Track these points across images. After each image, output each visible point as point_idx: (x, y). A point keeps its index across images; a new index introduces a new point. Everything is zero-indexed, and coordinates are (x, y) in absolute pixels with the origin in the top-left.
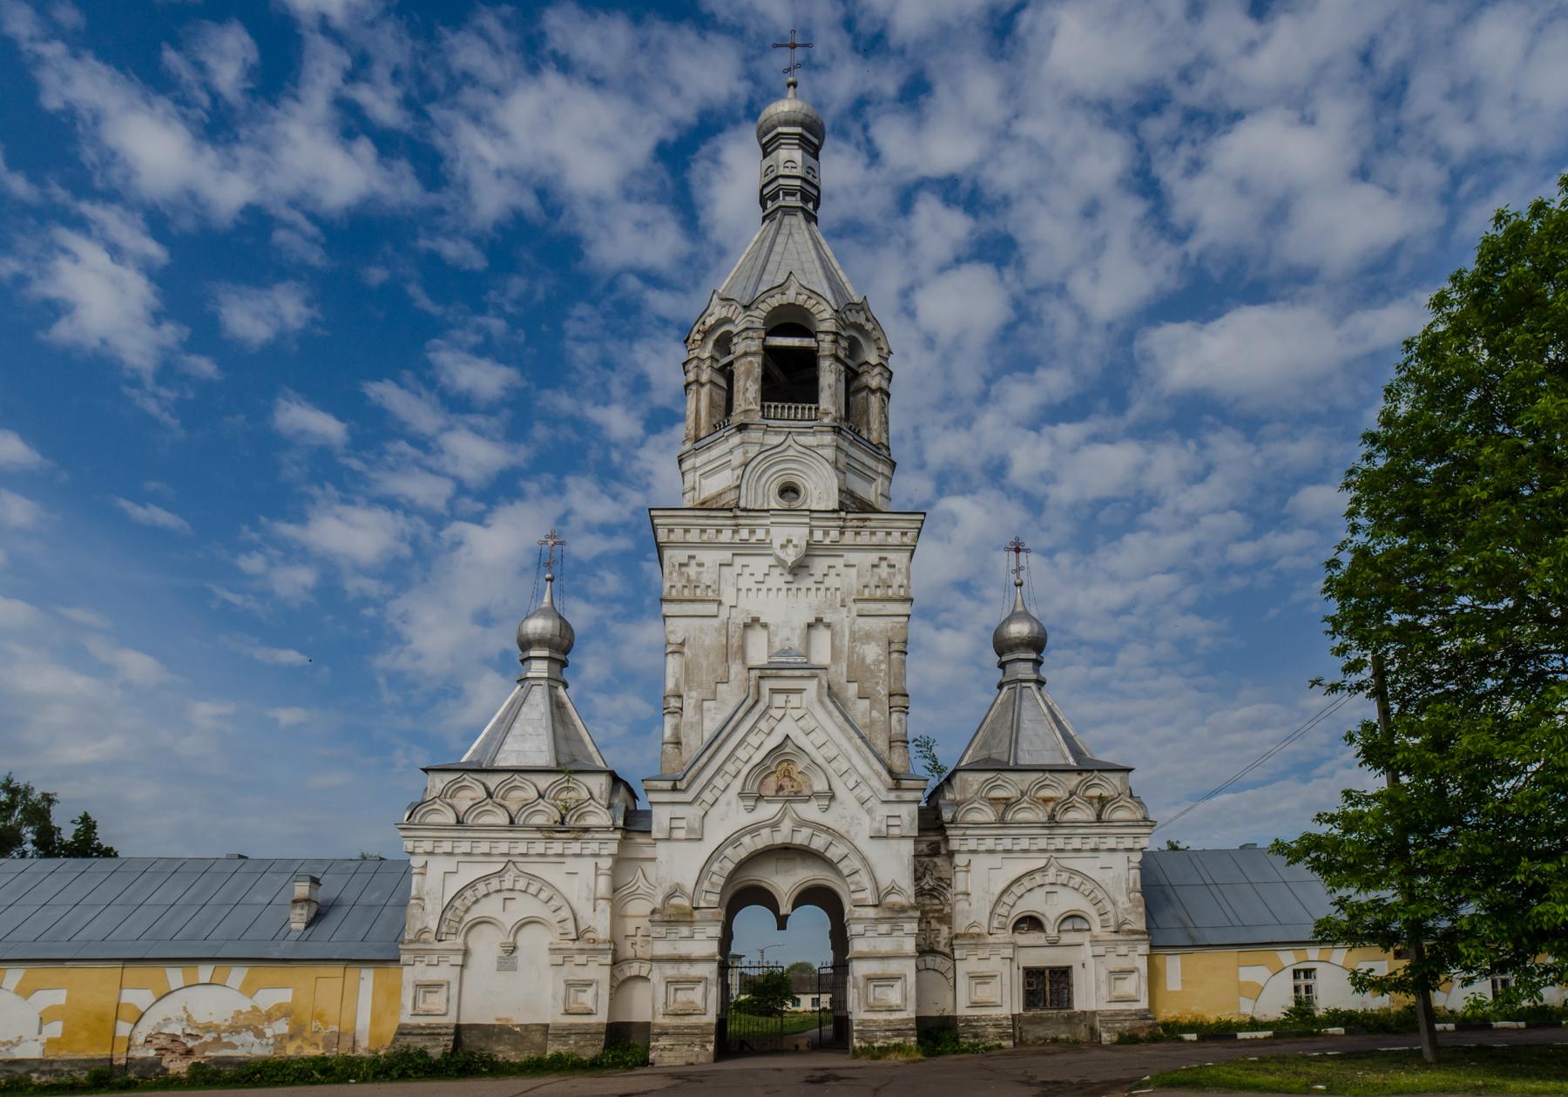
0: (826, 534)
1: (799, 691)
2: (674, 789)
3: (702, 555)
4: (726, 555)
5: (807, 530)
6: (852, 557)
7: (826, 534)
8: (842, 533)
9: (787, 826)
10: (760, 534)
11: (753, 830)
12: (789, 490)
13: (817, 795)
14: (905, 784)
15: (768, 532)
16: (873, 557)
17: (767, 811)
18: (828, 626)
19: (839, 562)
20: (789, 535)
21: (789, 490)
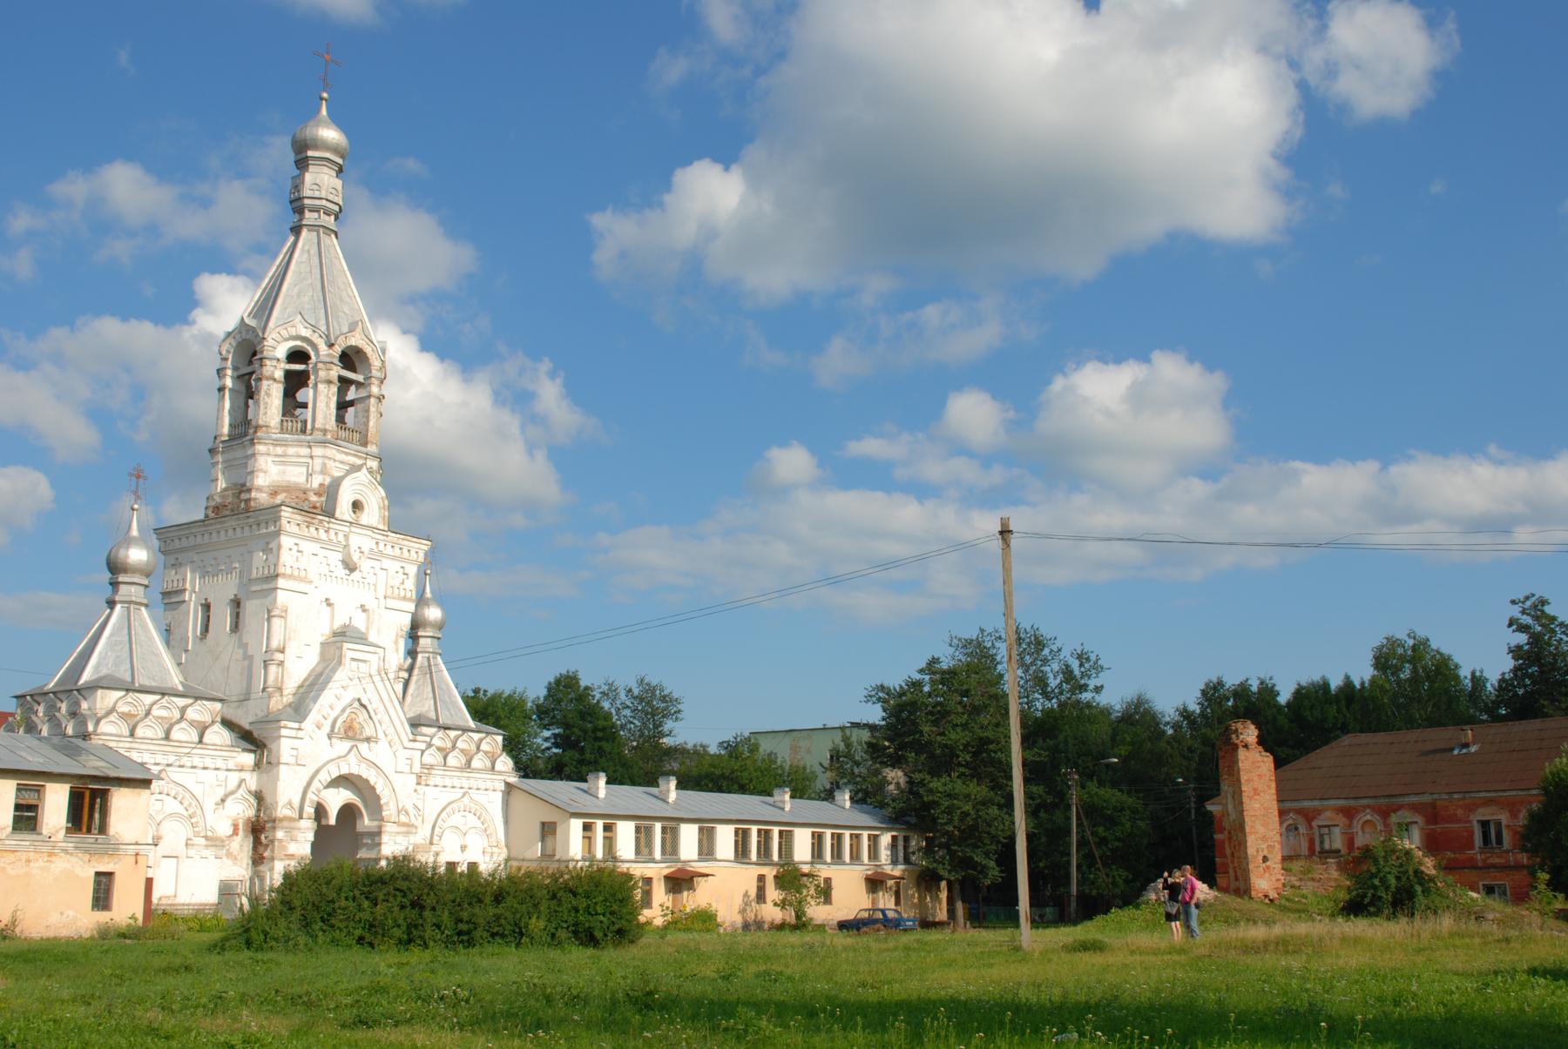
3: (304, 545)
4: (315, 547)
6: (386, 563)
12: (357, 506)
13: (368, 740)
15: (346, 537)
16: (397, 565)
17: (343, 746)
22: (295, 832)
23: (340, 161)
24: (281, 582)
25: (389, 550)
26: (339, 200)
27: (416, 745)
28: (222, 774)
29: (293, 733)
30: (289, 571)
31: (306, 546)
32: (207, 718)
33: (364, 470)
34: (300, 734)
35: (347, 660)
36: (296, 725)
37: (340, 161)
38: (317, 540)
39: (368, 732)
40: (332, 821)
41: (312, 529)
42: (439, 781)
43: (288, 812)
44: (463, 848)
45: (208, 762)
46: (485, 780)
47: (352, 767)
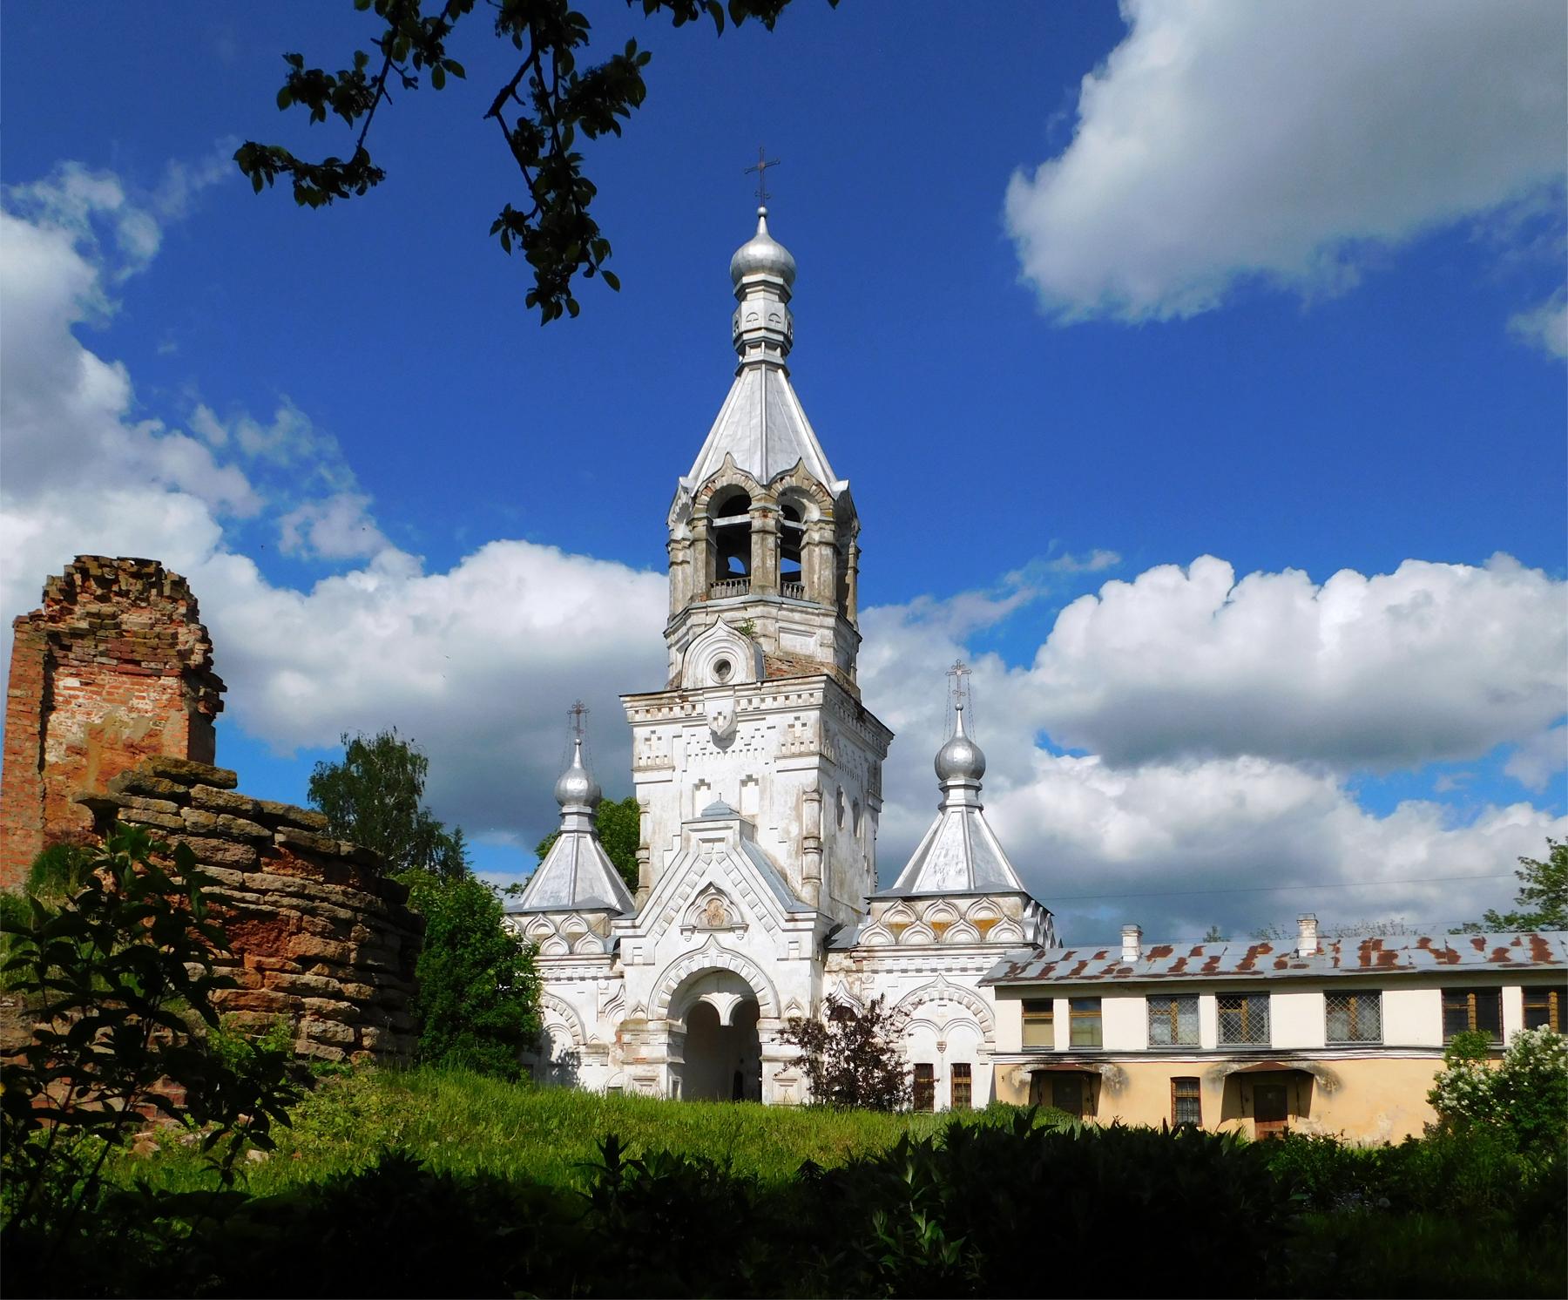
0: (750, 701)
1: (721, 840)
2: (634, 927)
5: (731, 701)
6: (771, 719)
7: (750, 701)
8: (763, 700)
9: (713, 952)
10: (699, 708)
11: (690, 954)
12: (723, 666)
14: (798, 916)
18: (756, 781)
19: (762, 725)
20: (717, 706)
21: (723, 666)
22: (644, 1036)
23: (780, 281)
24: (638, 777)
25: (769, 703)
26: (783, 327)
27: (800, 925)
28: (603, 983)
29: (630, 932)
30: (642, 763)
31: (666, 731)
32: (583, 929)
33: (720, 624)
34: (639, 932)
35: (693, 842)
36: (628, 923)
37: (780, 281)
38: (675, 721)
39: (736, 918)
40: (725, 1020)
41: (665, 710)
42: (888, 964)
43: (640, 1015)
44: (941, 1047)
45: (581, 972)
46: (971, 957)
47: (712, 959)
